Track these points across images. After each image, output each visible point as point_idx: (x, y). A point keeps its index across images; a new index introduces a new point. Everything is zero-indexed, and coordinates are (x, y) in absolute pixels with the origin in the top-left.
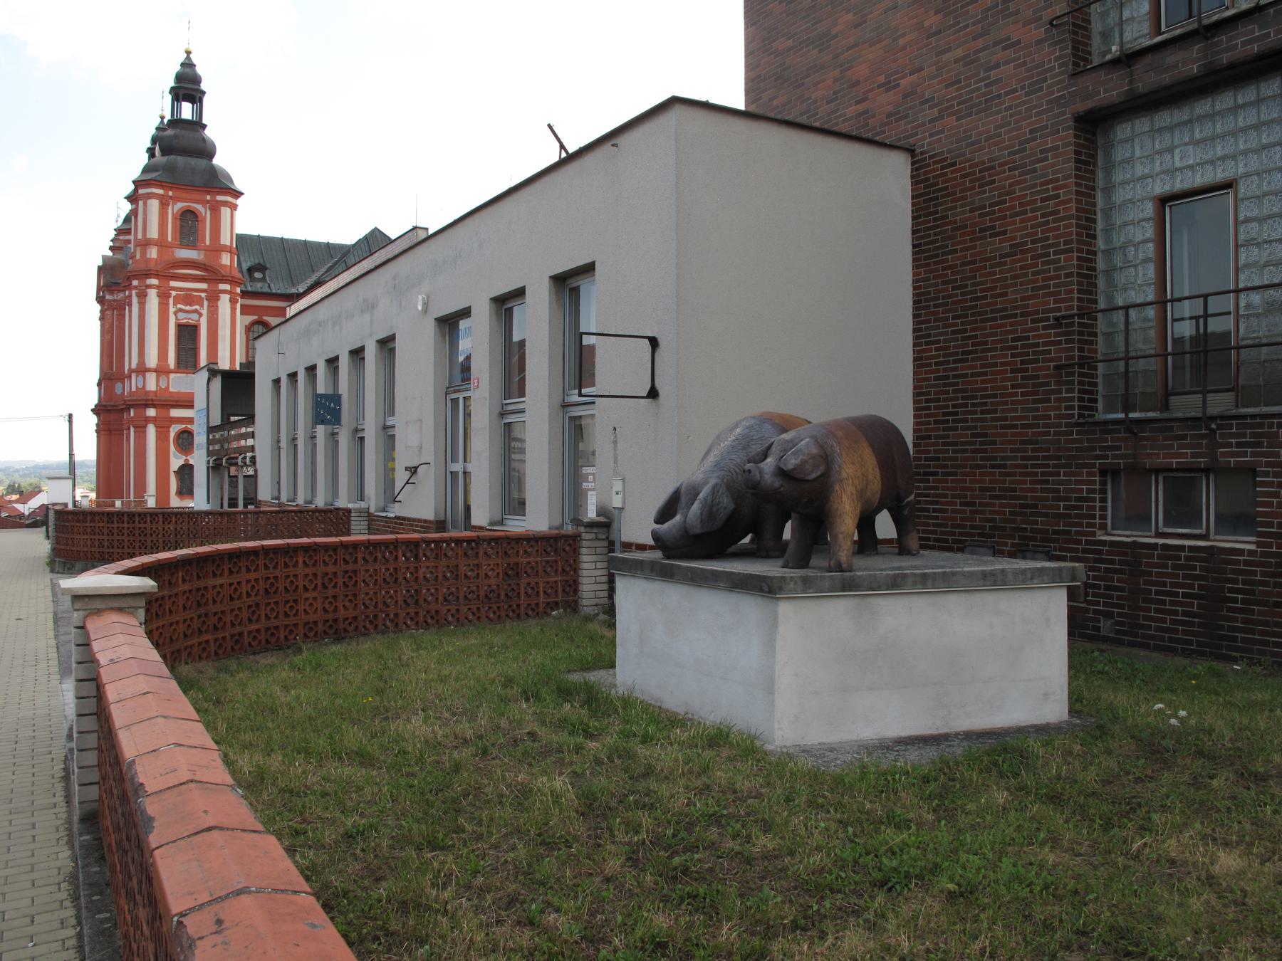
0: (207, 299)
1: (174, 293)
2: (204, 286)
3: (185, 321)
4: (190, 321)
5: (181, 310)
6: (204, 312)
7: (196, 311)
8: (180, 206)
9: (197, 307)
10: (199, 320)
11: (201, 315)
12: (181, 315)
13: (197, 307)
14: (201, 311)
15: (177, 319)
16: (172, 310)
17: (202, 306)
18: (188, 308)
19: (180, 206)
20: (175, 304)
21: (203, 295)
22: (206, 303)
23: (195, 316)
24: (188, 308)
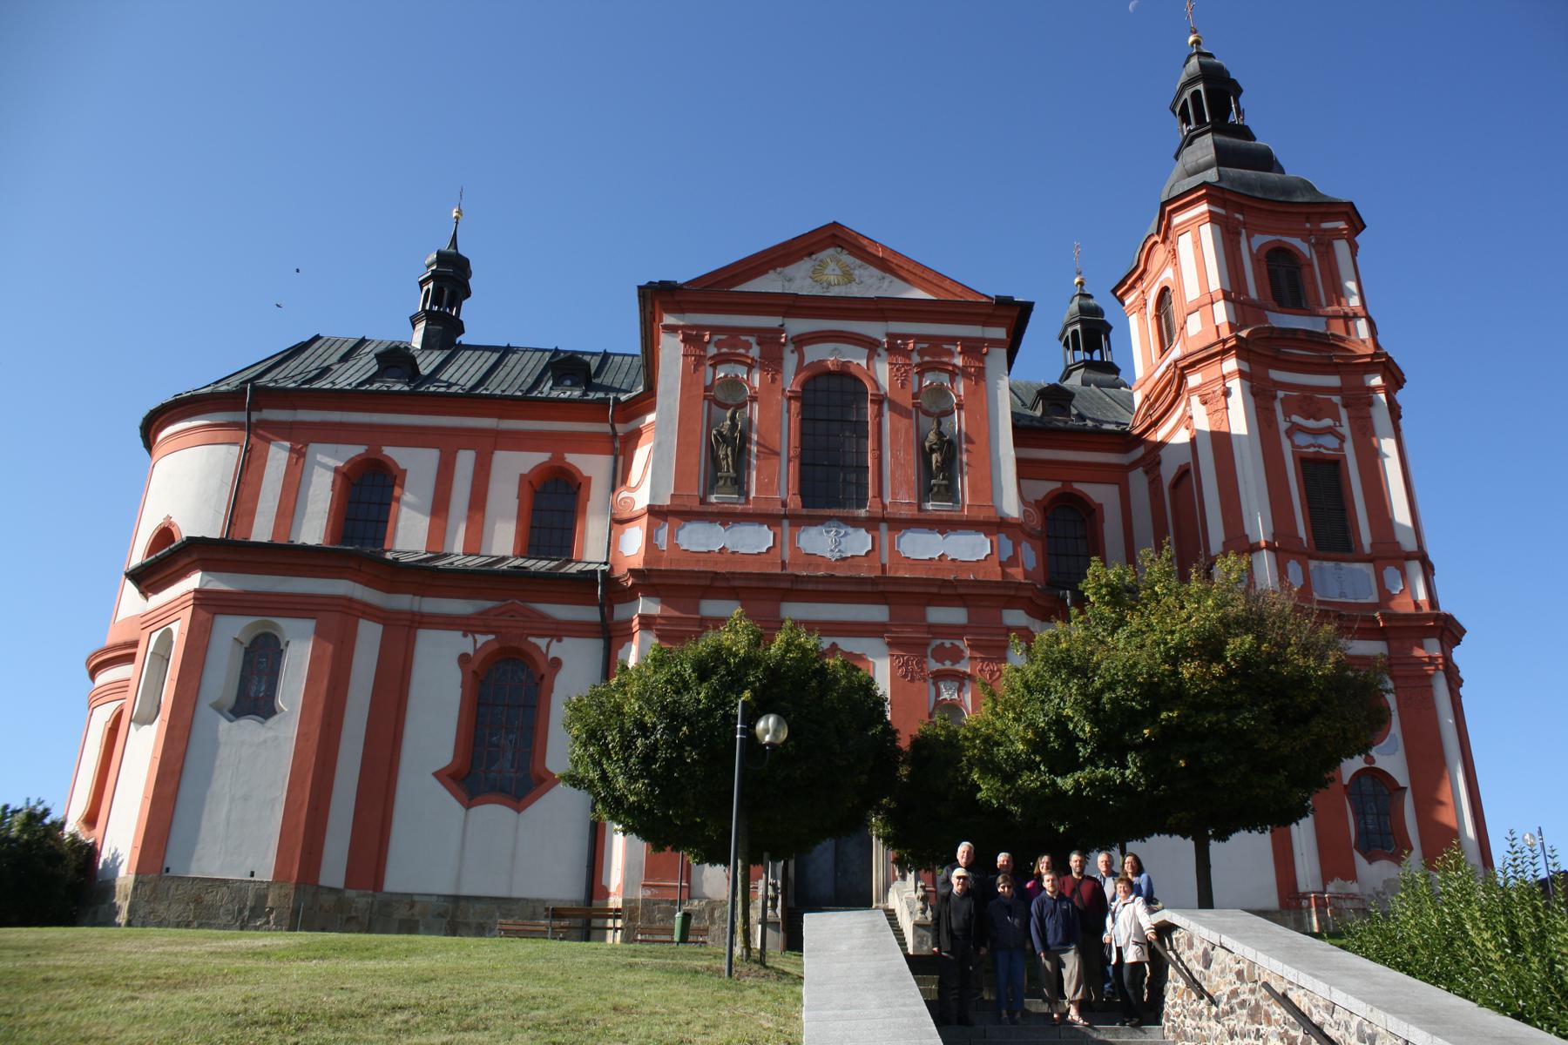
0: (1346, 406)
1: (1281, 394)
2: (1334, 381)
3: (1312, 450)
4: (1322, 450)
5: (1294, 429)
6: (1345, 430)
7: (1330, 431)
8: (1260, 240)
9: (1328, 422)
10: (1341, 449)
11: (1342, 438)
12: (1302, 439)
13: (1328, 422)
14: (1339, 429)
15: (1293, 445)
16: (1283, 425)
17: (1337, 418)
18: (1311, 423)
19: (1260, 240)
20: (1287, 415)
21: (1336, 399)
22: (1343, 413)
23: (1330, 442)
24: (1311, 423)
